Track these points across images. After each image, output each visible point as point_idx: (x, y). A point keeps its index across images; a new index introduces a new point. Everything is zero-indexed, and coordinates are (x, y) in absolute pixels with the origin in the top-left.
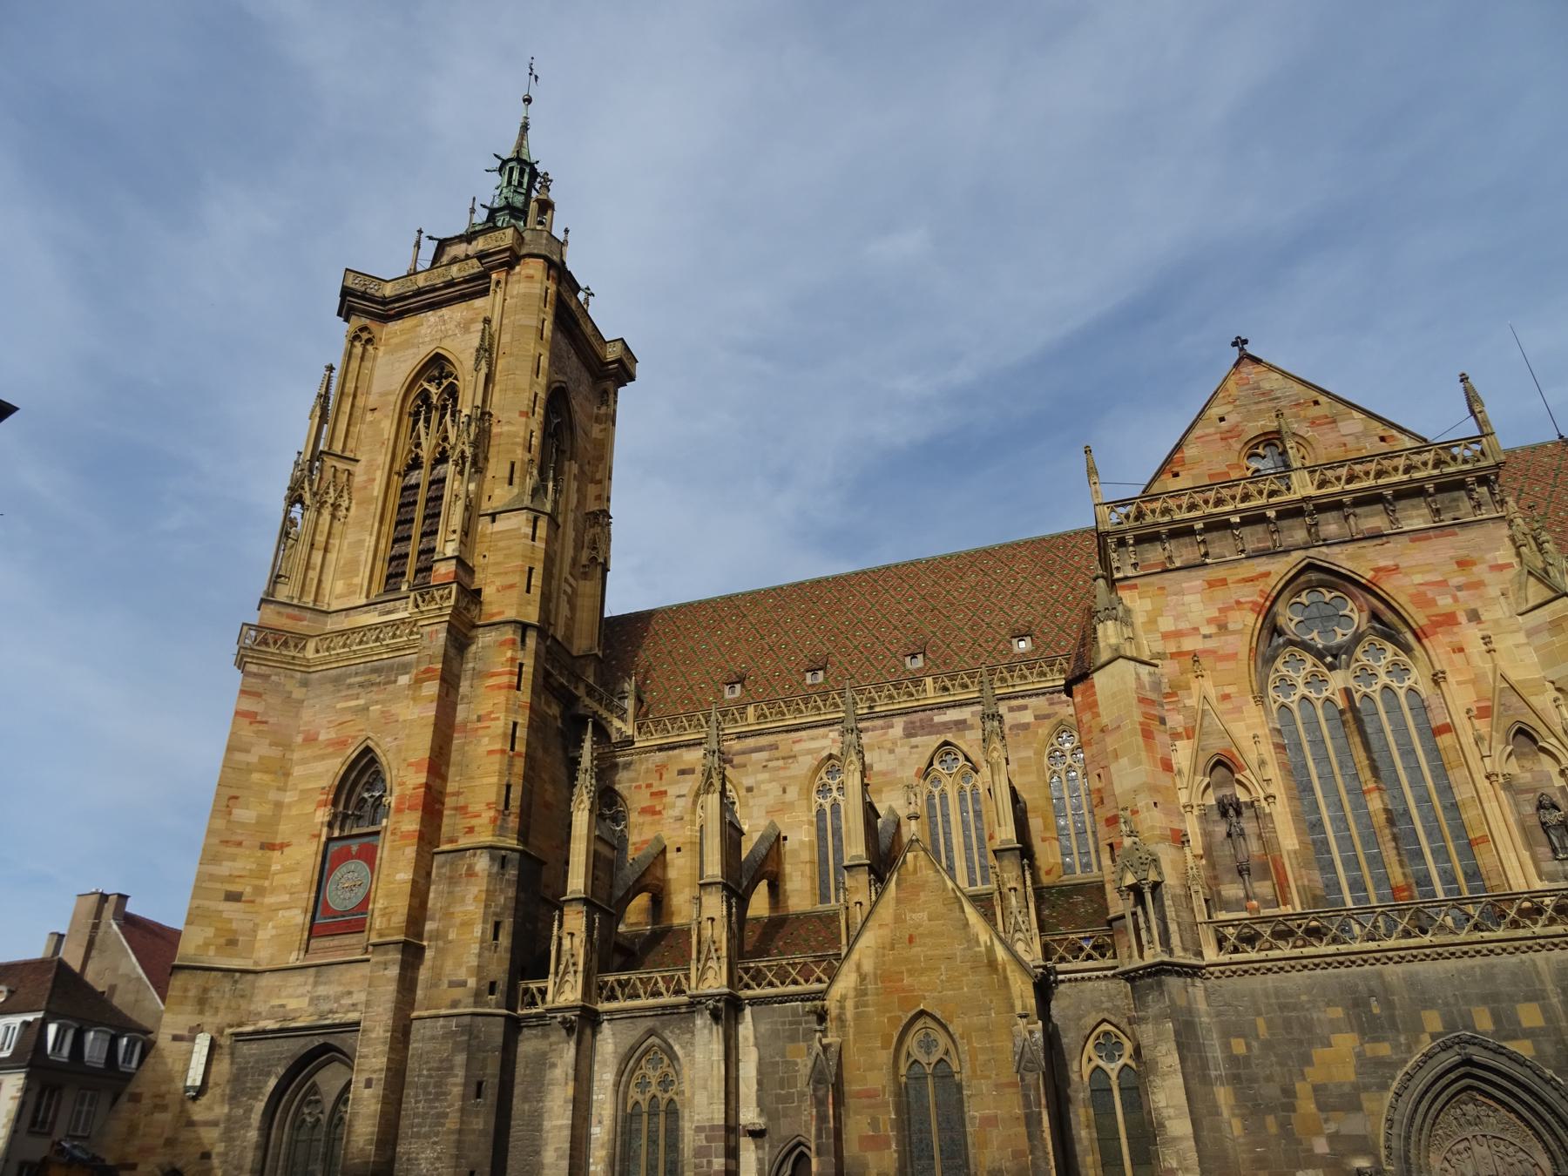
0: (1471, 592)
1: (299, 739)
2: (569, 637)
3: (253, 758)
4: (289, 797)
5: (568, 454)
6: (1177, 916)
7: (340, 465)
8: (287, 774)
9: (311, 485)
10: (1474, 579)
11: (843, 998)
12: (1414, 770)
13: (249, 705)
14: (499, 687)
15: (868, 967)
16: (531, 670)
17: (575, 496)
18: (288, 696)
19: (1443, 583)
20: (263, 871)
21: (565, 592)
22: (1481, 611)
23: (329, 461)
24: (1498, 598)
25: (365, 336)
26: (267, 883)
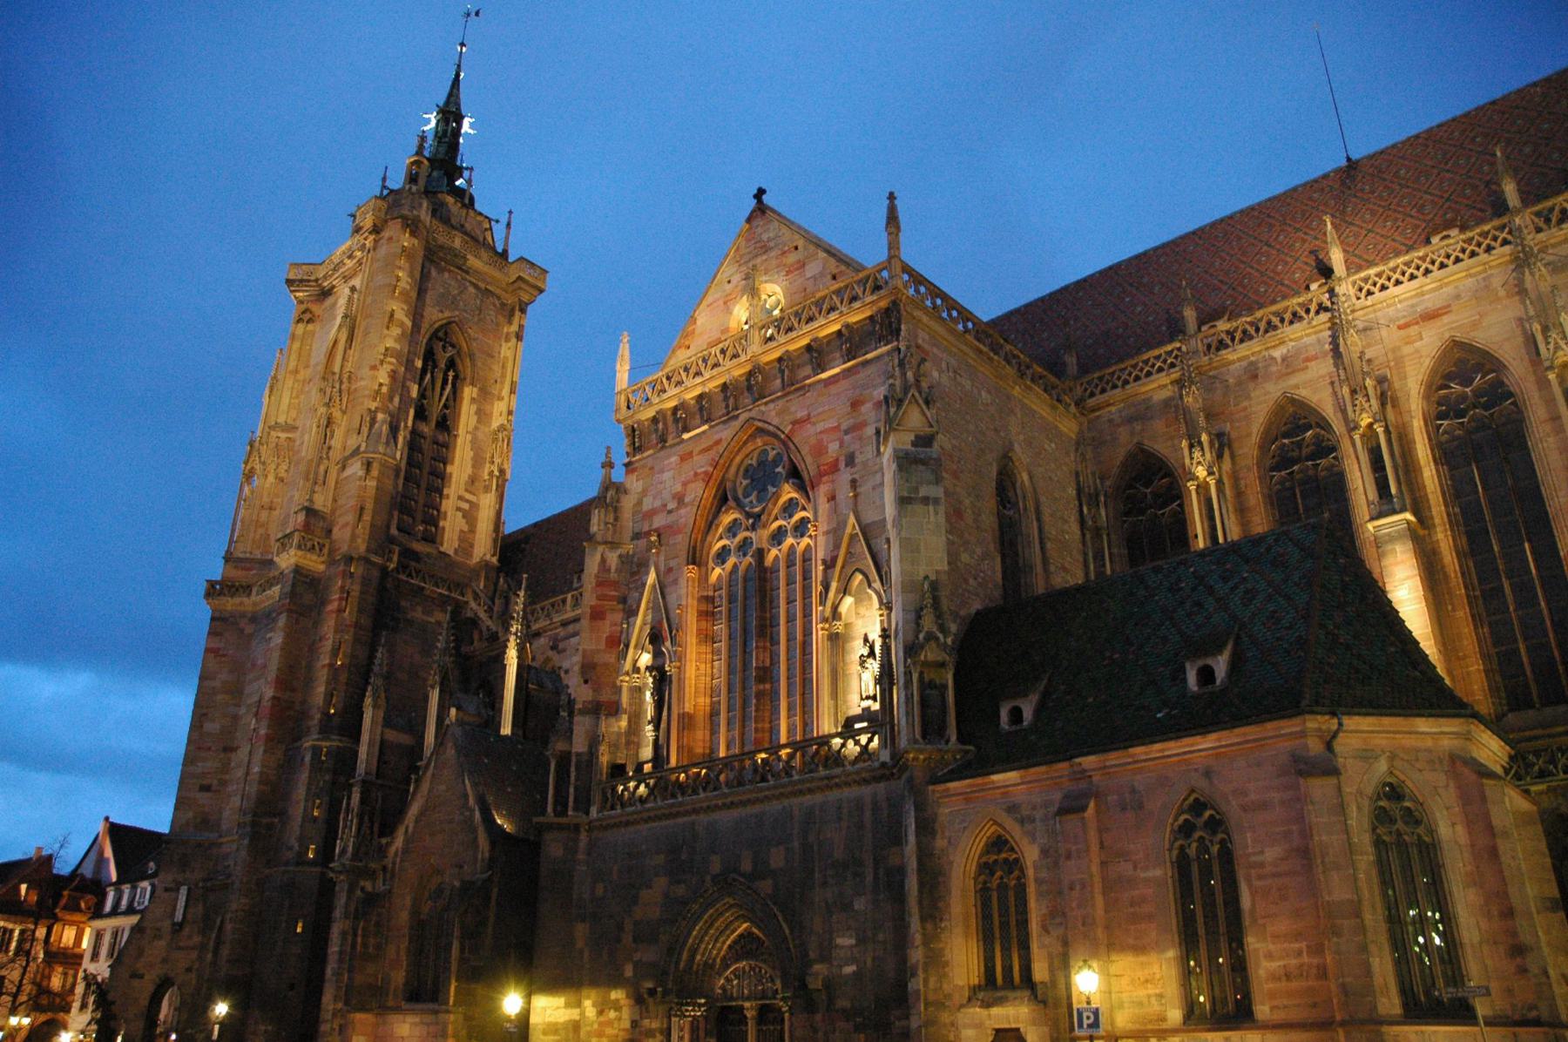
0: (854, 434)
1: (249, 665)
2: (466, 543)
3: (217, 684)
4: (243, 711)
5: (468, 381)
6: (576, 780)
7: (283, 435)
8: (241, 692)
9: (260, 457)
10: (861, 419)
11: (396, 854)
12: (790, 619)
13: (216, 644)
14: (332, 611)
15: (410, 830)
16: (357, 594)
17: (473, 420)
18: (242, 631)
19: (837, 428)
20: (225, 768)
21: (459, 509)
22: (857, 454)
23: (273, 434)
24: (870, 437)
25: (307, 316)
26: (227, 777)
